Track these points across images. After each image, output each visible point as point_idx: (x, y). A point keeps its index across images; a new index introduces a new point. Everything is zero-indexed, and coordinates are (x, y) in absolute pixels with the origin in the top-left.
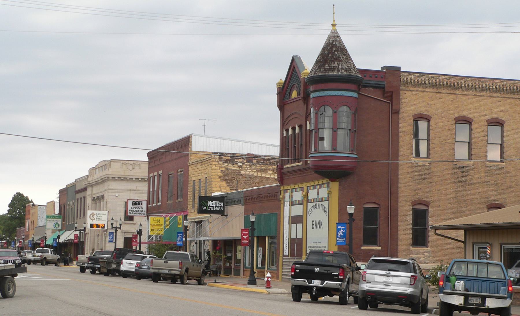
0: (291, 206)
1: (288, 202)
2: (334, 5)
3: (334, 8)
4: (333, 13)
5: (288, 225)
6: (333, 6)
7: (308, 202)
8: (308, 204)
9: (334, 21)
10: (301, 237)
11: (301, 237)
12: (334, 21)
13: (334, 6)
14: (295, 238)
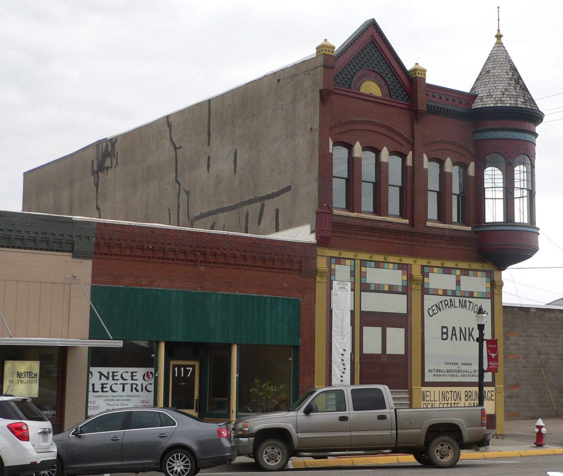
0: (362, 290)
1: (349, 284)
2: (498, 8)
3: (498, 11)
4: (497, 19)
5: (349, 329)
6: (497, 9)
7: (425, 291)
8: (426, 296)
9: (499, 30)
10: (402, 352)
11: (402, 352)
12: (499, 30)
13: (499, 9)
14: (380, 352)
